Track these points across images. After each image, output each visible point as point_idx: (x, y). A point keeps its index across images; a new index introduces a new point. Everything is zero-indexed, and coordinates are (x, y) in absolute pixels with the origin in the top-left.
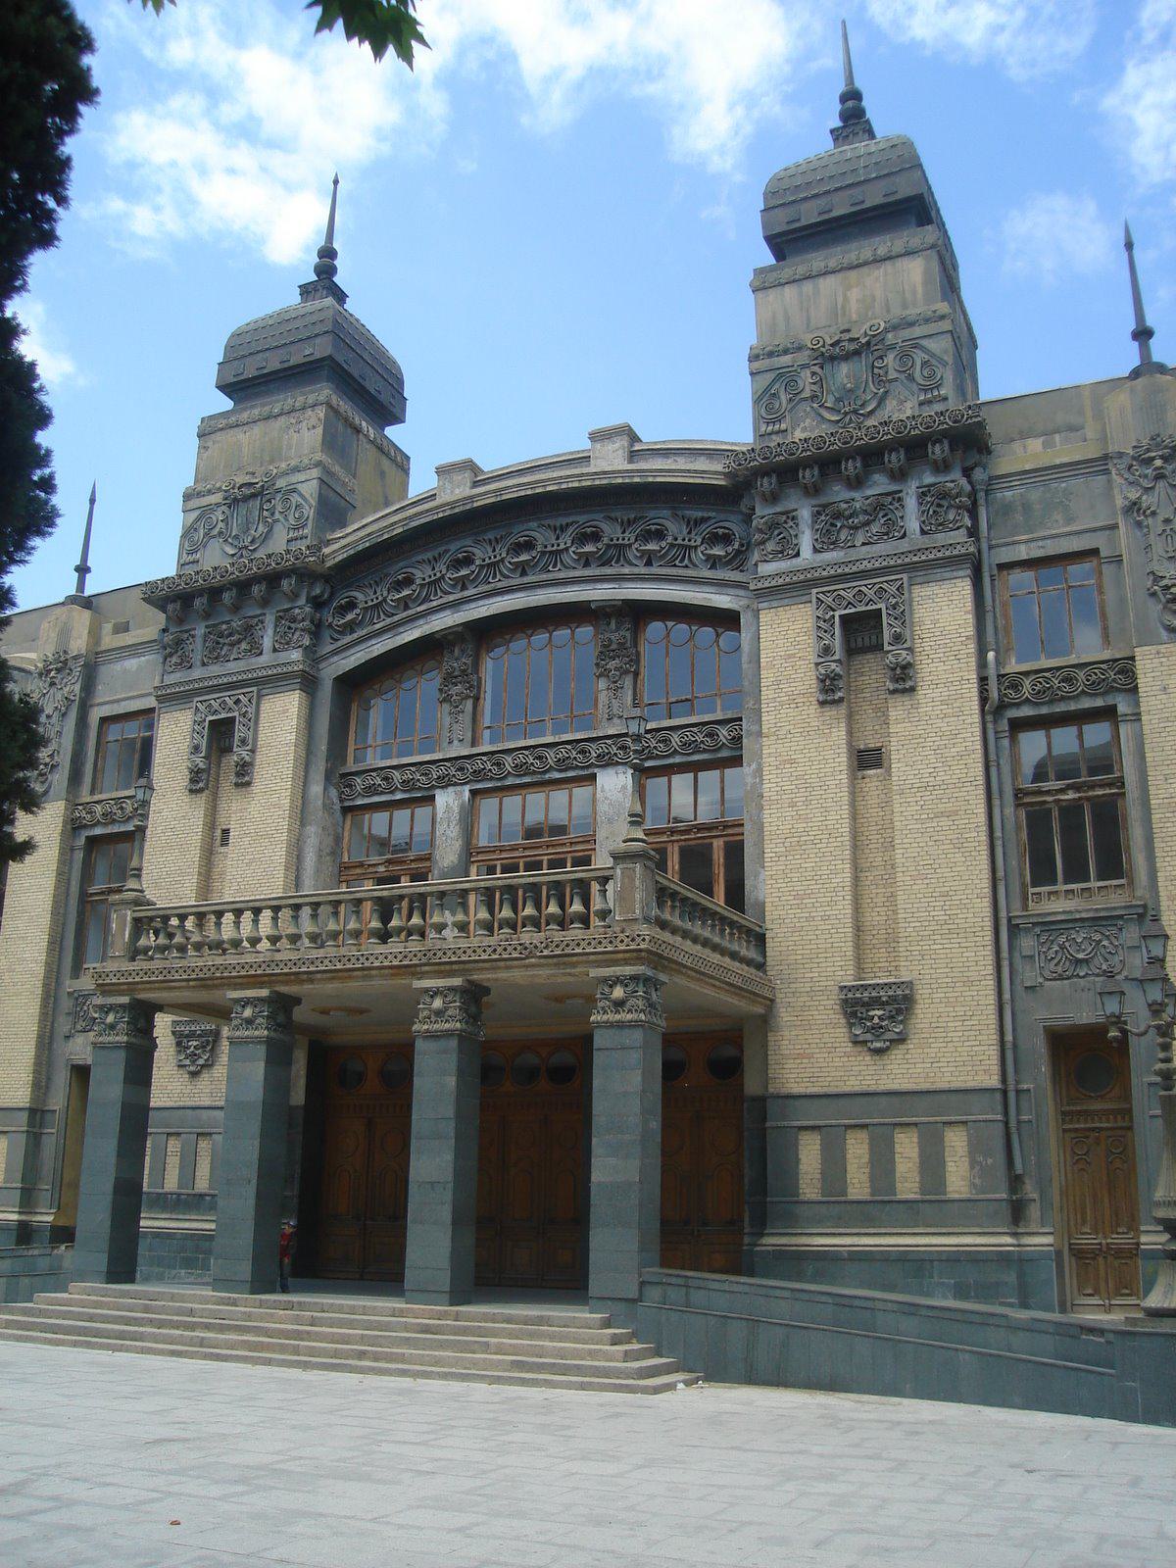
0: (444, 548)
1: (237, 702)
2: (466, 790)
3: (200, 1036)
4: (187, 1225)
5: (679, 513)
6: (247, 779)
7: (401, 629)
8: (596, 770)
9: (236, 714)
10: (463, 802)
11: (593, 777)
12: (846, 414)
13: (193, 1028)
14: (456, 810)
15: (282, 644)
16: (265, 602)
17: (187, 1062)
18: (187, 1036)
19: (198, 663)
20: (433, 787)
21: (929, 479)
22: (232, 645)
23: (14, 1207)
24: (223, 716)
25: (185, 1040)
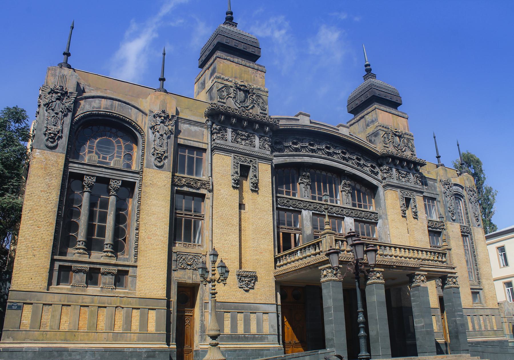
0: (304, 137)
1: (251, 161)
2: (311, 212)
3: (250, 277)
4: (236, 346)
5: (364, 156)
6: (257, 189)
7: (295, 157)
8: (345, 216)
9: (250, 165)
10: (310, 216)
11: (344, 218)
12: (399, 149)
13: (247, 274)
14: (309, 217)
15: (262, 147)
16: (256, 131)
17: (244, 286)
18: (244, 277)
19: (231, 141)
20: (302, 208)
21: (414, 172)
22: (242, 139)
23: (163, 342)
24: (245, 164)
25: (243, 278)
